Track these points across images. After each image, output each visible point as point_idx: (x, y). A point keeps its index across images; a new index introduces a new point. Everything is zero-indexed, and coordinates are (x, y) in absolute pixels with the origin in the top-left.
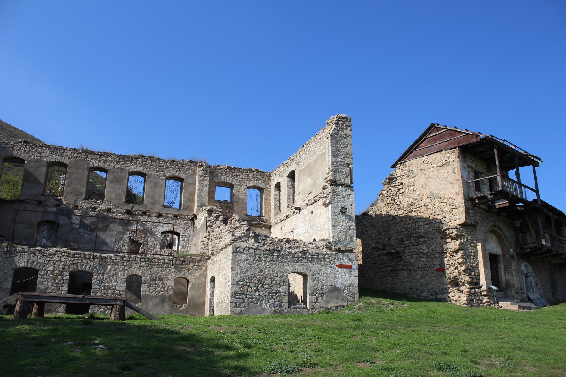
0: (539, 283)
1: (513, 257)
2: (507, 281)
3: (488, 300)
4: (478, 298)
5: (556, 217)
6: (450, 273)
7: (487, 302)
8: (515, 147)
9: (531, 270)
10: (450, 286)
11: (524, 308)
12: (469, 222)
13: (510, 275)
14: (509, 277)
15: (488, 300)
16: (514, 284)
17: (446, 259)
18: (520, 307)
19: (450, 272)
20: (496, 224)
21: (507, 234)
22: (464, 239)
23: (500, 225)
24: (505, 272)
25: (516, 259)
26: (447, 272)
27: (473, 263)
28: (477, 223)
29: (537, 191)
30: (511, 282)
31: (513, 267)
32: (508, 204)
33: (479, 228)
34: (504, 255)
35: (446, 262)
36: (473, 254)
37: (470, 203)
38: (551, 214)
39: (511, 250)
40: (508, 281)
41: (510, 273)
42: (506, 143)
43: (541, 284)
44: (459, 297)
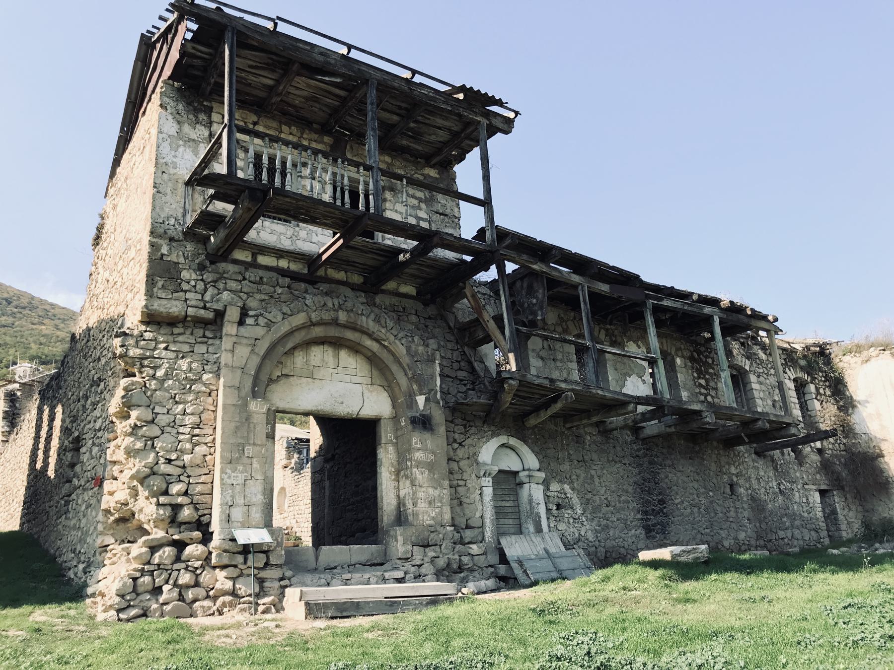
0: (575, 500)
1: (423, 423)
2: (401, 504)
3: (229, 585)
4: (185, 578)
5: (604, 288)
6: (111, 494)
7: (225, 593)
8: (350, 47)
9: (532, 461)
10: (109, 540)
11: (344, 610)
12: (175, 308)
13: (408, 482)
14: (406, 490)
15: (229, 585)
16: (415, 515)
17: (113, 444)
18: (313, 610)
19: (115, 493)
20: (342, 317)
21: (401, 350)
22: (155, 368)
23: (369, 323)
24: (397, 473)
25: (442, 430)
26: (108, 486)
27: (183, 452)
28: (220, 315)
29: (486, 203)
30: (409, 505)
31: (418, 455)
32: (341, 241)
33: (230, 328)
34: (395, 418)
35: (108, 458)
36: (189, 420)
37: (190, 247)
38: (576, 278)
39: (421, 400)
40: (404, 505)
41: (407, 478)
42: (282, 28)
43: (586, 502)
44: (112, 575)
